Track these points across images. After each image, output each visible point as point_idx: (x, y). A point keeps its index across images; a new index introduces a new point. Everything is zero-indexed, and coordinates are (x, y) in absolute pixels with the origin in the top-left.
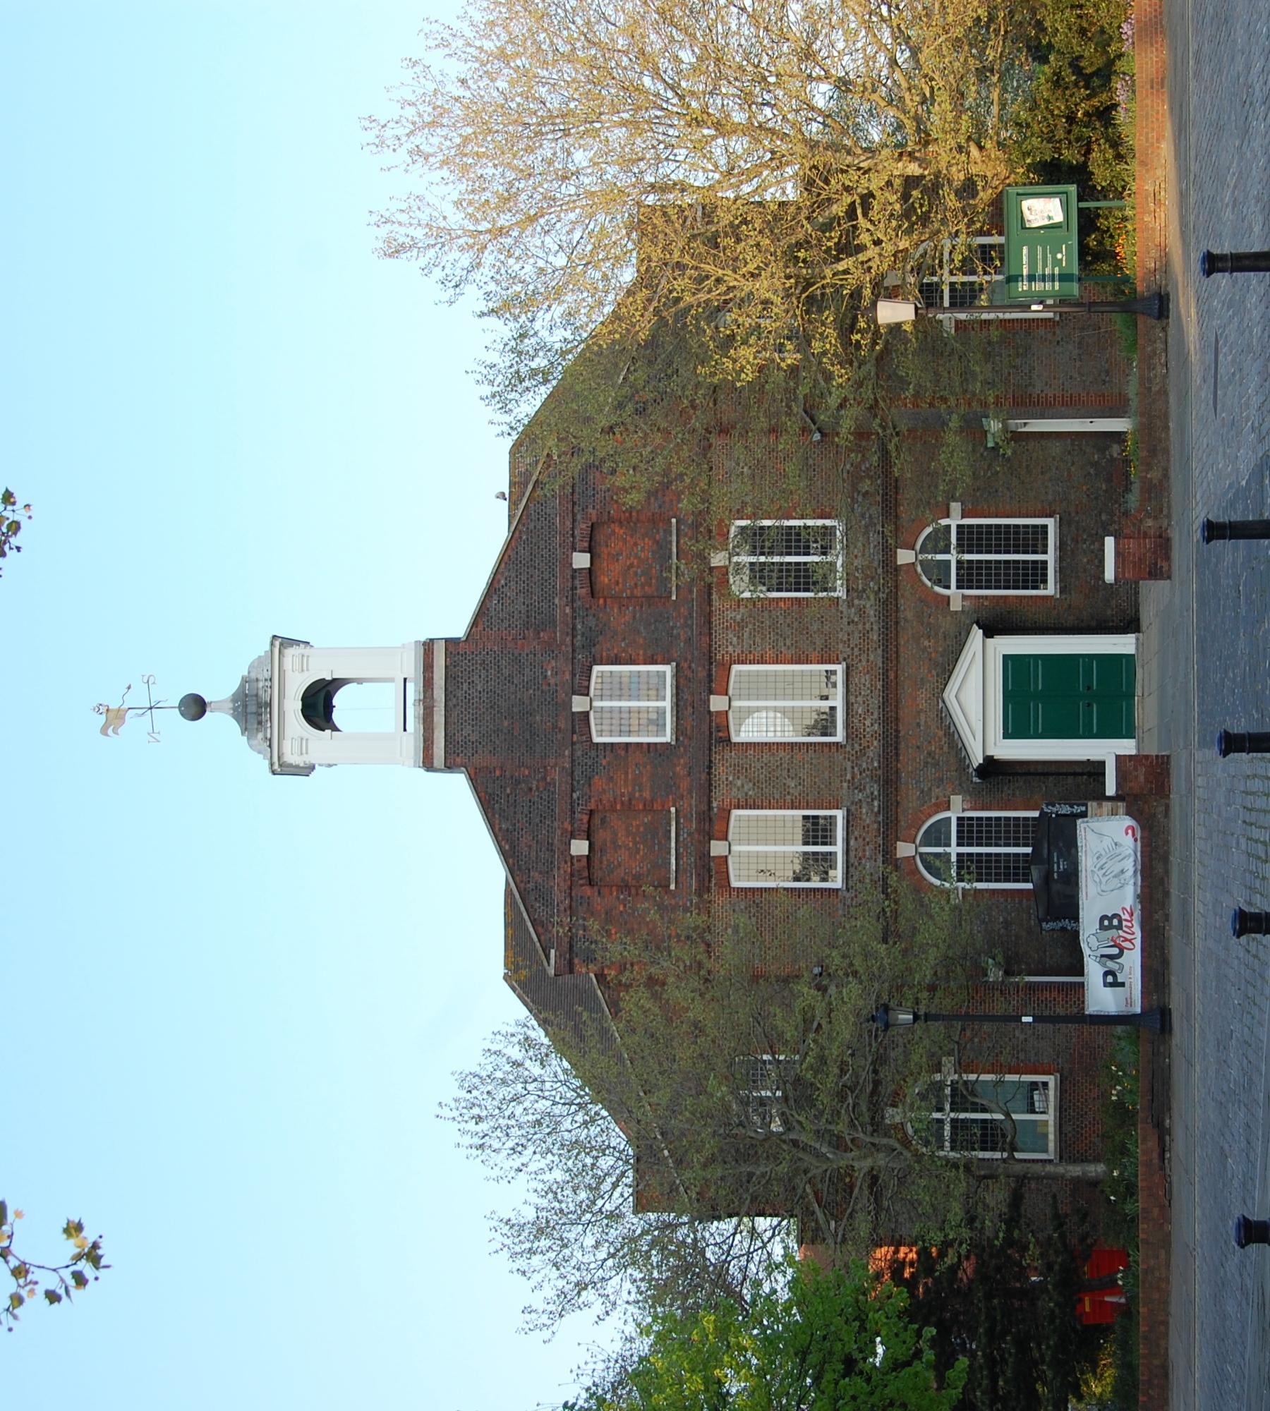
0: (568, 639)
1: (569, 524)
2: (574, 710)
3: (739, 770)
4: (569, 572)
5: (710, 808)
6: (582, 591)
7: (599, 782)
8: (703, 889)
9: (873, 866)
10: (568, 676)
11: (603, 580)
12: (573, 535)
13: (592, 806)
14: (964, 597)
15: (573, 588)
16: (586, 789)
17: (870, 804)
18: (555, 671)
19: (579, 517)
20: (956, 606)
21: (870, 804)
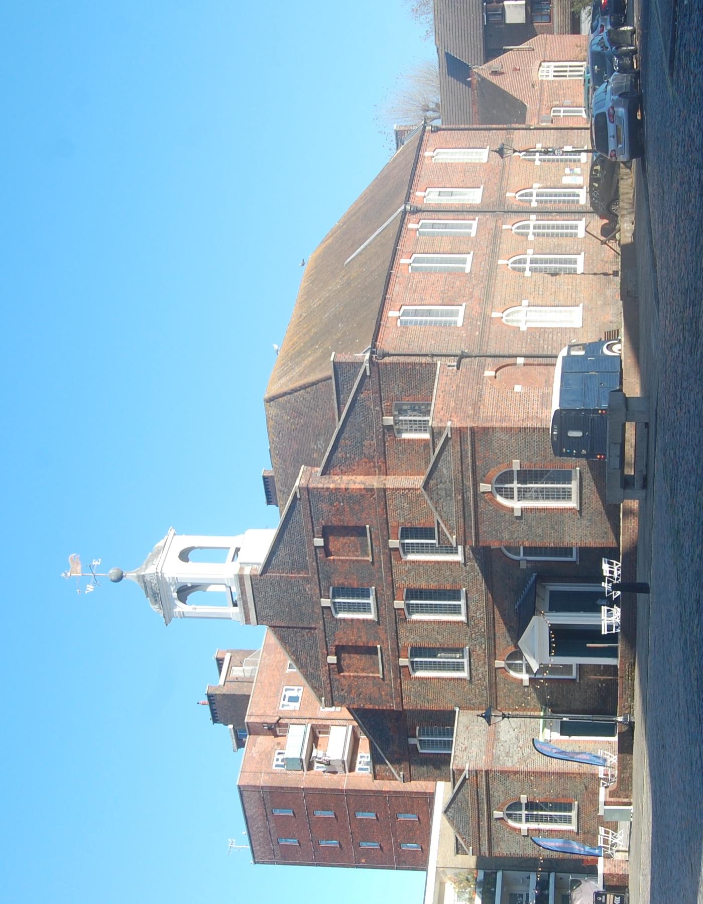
0: (316, 576)
1: (310, 527)
2: (323, 605)
3: (410, 631)
4: (313, 548)
5: (398, 646)
6: (321, 555)
7: (340, 633)
8: (398, 677)
9: (483, 670)
10: (318, 591)
11: (332, 548)
12: (313, 531)
13: (337, 643)
14: (528, 561)
15: (316, 554)
16: (332, 637)
17: (481, 647)
18: (311, 589)
19: (315, 523)
20: (523, 565)
21: (481, 647)
